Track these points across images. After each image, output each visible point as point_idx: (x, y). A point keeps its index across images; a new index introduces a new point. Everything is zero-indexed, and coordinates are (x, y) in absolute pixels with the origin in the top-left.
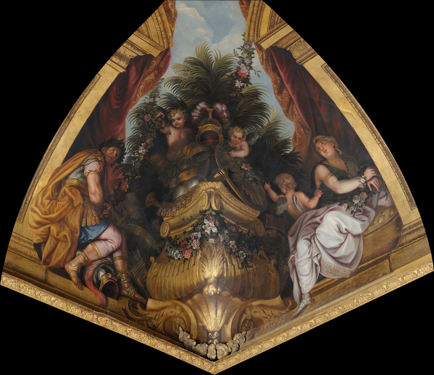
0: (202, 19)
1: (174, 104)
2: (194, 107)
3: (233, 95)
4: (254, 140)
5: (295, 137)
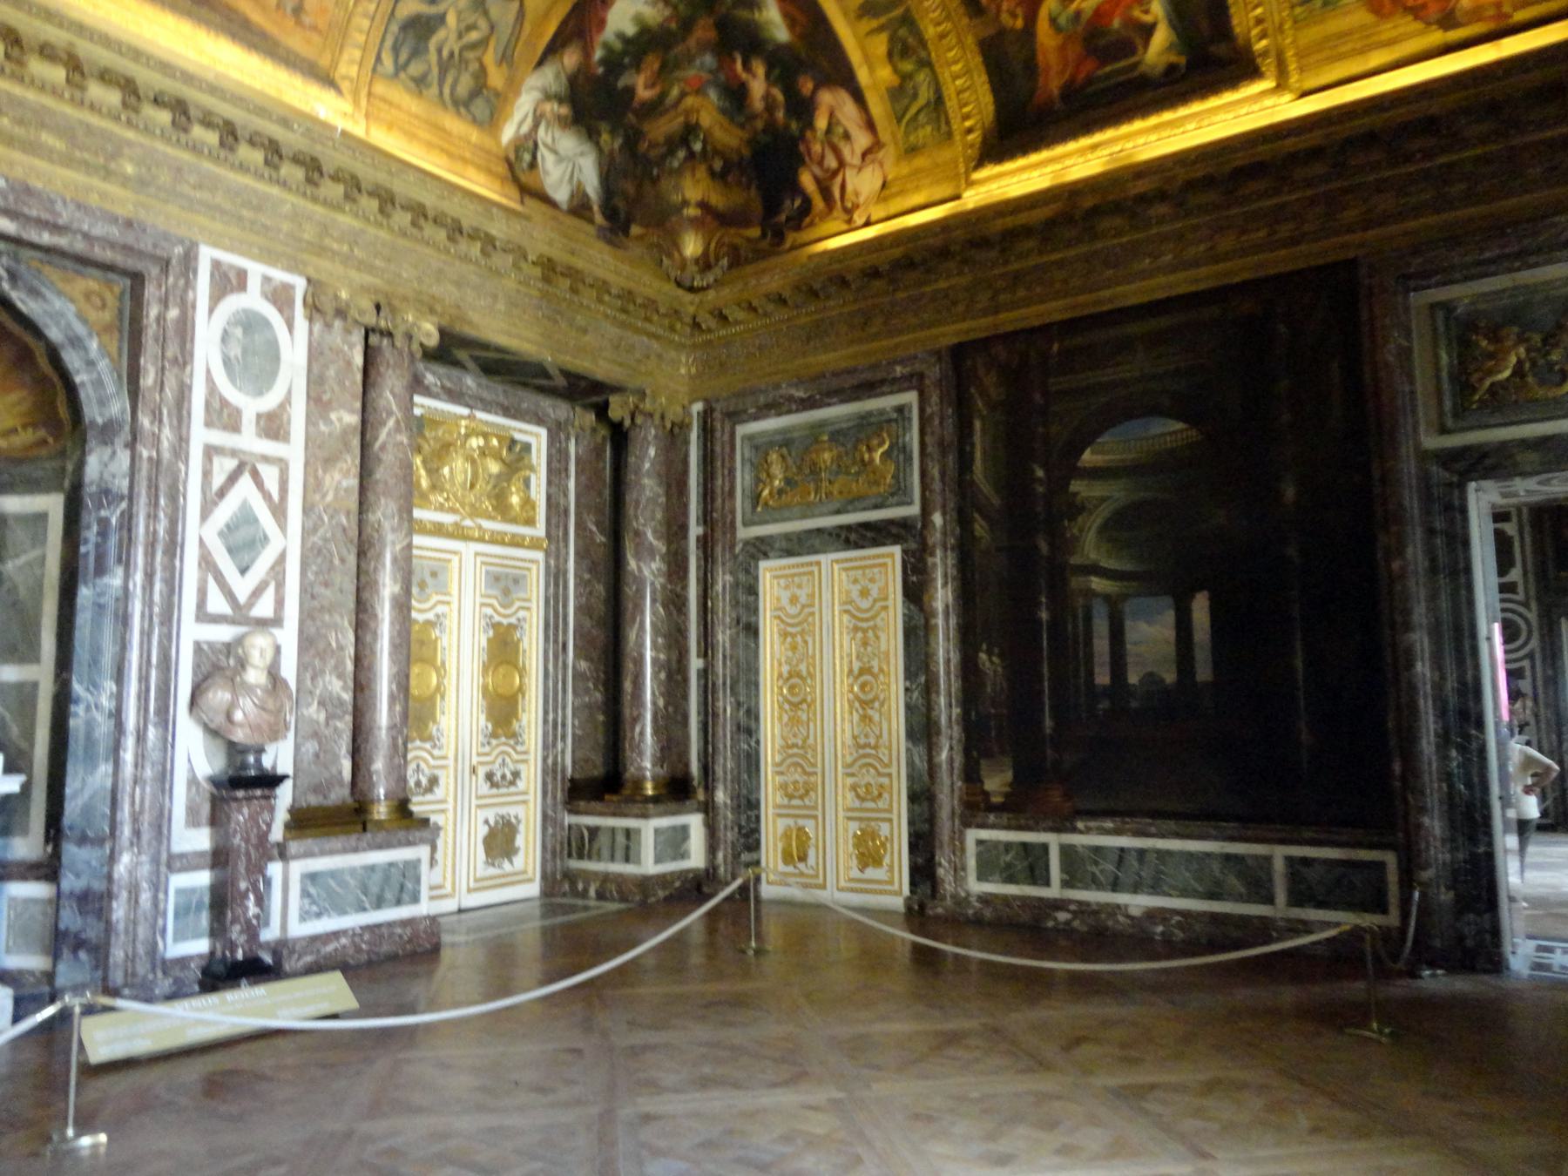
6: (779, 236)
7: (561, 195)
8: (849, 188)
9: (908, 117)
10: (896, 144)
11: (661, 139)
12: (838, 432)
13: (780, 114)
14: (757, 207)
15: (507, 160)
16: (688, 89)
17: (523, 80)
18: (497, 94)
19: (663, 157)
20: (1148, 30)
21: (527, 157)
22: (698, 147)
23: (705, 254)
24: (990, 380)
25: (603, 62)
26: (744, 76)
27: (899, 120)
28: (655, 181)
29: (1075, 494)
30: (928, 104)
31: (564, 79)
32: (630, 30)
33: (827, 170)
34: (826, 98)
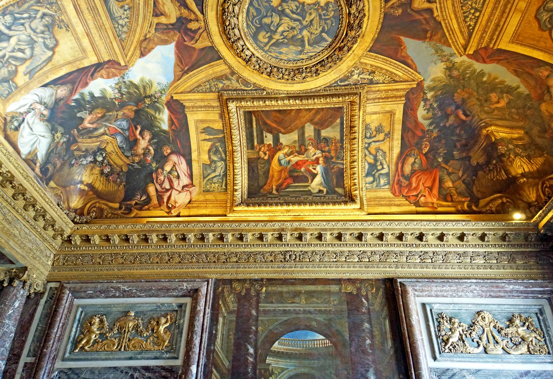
6: (129, 210)
7: (25, 150)
8: (172, 198)
9: (207, 178)
10: (200, 187)
11: (84, 149)
12: (142, 312)
13: (149, 158)
14: (122, 195)
15: (5, 119)
16: (108, 132)
17: (32, 88)
18: (17, 87)
19: (80, 157)
20: (314, 176)
21: (16, 124)
22: (100, 159)
23: (83, 208)
24: (231, 299)
25: (76, 100)
26: (139, 137)
27: (204, 178)
28: (72, 165)
29: (269, 364)
30: (220, 175)
31: (54, 99)
32: (97, 94)
33: (165, 188)
34: (174, 158)
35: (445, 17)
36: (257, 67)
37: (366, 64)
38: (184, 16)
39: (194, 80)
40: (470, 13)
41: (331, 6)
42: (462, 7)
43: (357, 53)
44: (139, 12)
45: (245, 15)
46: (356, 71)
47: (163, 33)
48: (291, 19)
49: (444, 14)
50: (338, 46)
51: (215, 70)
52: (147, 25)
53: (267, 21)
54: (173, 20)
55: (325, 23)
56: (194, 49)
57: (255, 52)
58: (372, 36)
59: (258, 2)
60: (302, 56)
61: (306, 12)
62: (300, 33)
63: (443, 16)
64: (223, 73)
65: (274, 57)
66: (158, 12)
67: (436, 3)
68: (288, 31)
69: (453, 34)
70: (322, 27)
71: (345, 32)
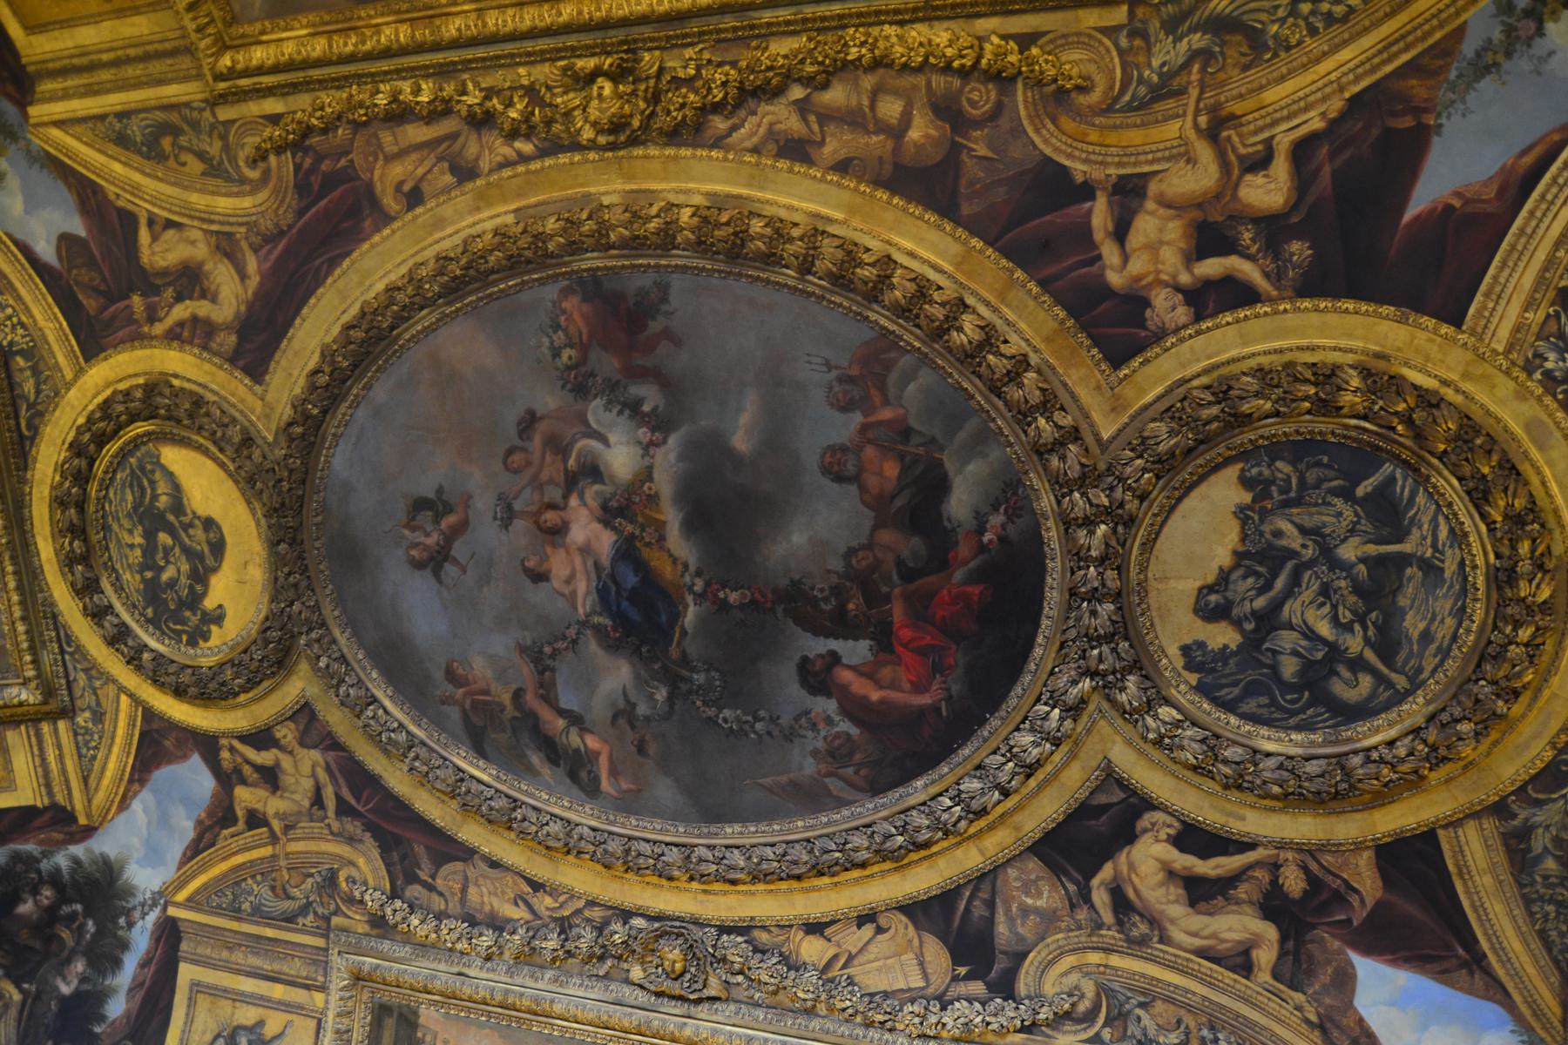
0: (145, 833)
1: (55, 879)
2: (69, 901)
3: (110, 925)
4: (86, 987)
5: (114, 1021)
35: (1328, 90)
36: (1465, 727)
37: (1517, 329)
38: (1256, 896)
39: (1515, 945)
40: (1313, 13)
41: (1254, 471)
42: (1288, 48)
43: (1460, 369)
44: (1230, 1010)
45: (1264, 731)
46: (1549, 365)
47: (1311, 973)
48: (1289, 593)
49: (1319, 95)
50: (1408, 443)
51: (1482, 864)
52: (1273, 1005)
53: (1289, 668)
54: (1270, 932)
55: (1317, 486)
56: (1379, 904)
57: (1408, 723)
58: (1385, 327)
59: (1226, 686)
60: (1450, 568)
61: (1270, 545)
62: (1347, 567)
63: (1324, 99)
64: (1497, 842)
65: (1442, 662)
66: (1239, 960)
67: (1273, 137)
68: (1335, 607)
69: (1403, 37)
70: (1329, 498)
71: (1354, 422)
